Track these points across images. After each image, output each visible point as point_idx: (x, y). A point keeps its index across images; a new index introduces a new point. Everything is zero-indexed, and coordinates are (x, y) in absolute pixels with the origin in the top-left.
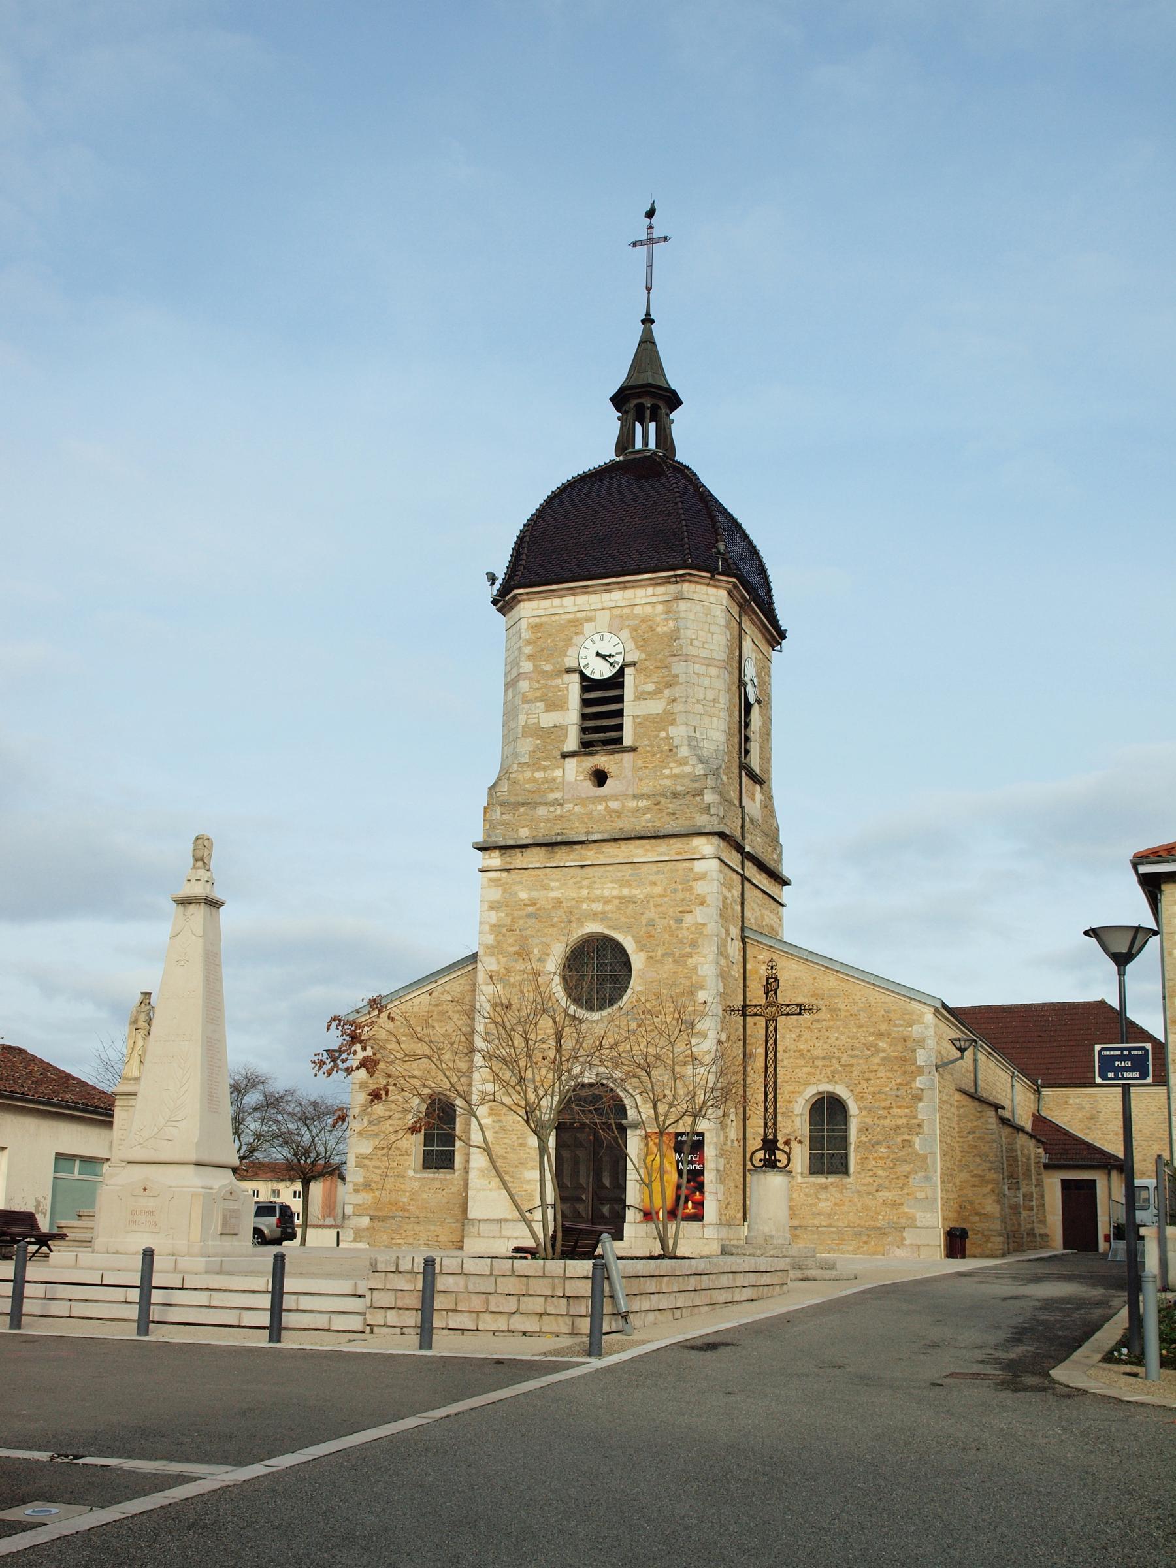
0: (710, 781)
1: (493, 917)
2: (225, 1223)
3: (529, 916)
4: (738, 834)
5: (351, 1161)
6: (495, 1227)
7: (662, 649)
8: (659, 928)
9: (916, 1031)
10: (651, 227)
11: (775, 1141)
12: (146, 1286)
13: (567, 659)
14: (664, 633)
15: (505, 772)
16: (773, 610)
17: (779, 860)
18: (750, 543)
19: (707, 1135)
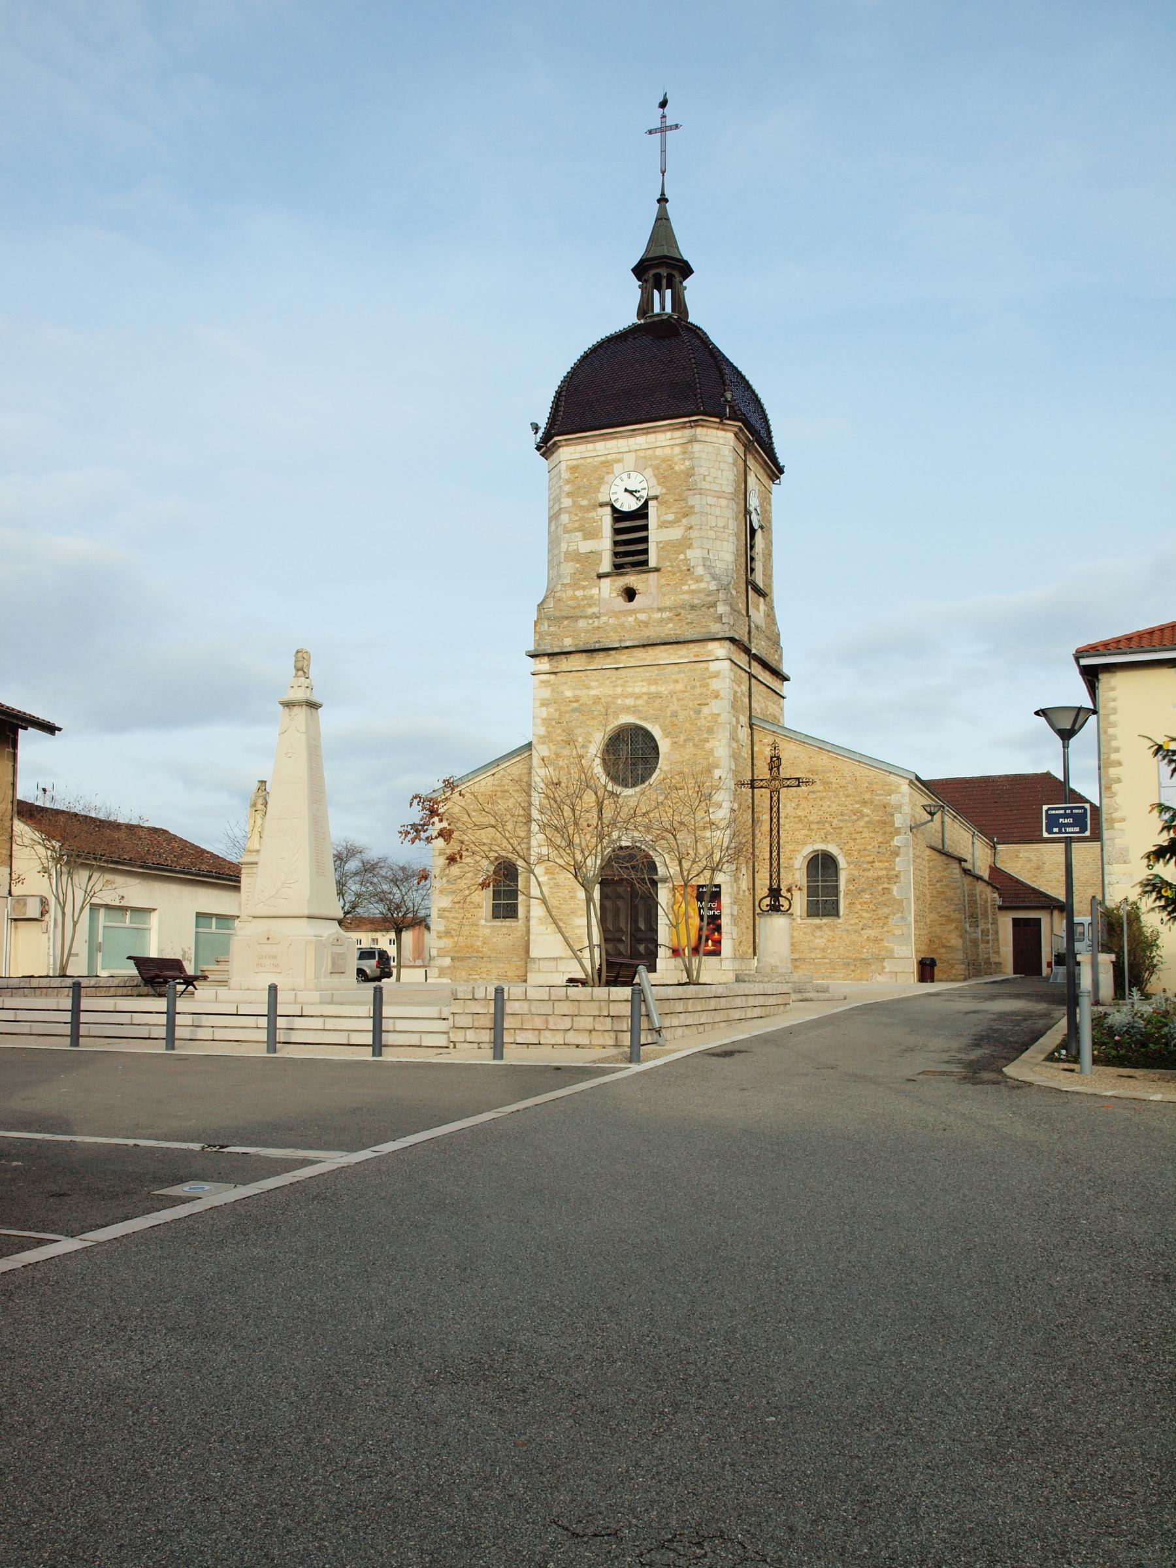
0: (722, 596)
1: (544, 712)
2: (334, 964)
3: (574, 710)
4: (746, 639)
5: (434, 913)
6: (553, 963)
7: (680, 483)
8: (681, 718)
9: (894, 799)
10: (664, 117)
11: (779, 890)
12: (272, 1015)
13: (600, 495)
14: (682, 471)
15: (551, 592)
16: (773, 449)
17: (780, 660)
18: (753, 392)
19: (723, 887)
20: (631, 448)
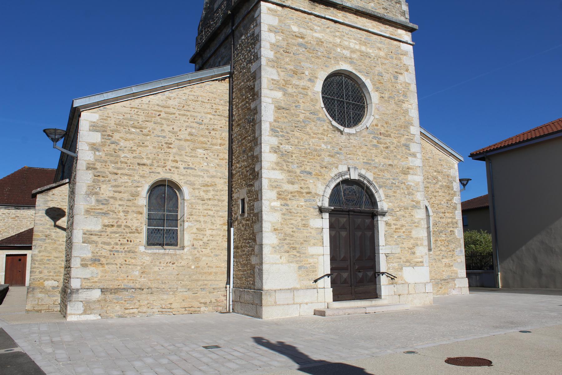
3: (300, 45)
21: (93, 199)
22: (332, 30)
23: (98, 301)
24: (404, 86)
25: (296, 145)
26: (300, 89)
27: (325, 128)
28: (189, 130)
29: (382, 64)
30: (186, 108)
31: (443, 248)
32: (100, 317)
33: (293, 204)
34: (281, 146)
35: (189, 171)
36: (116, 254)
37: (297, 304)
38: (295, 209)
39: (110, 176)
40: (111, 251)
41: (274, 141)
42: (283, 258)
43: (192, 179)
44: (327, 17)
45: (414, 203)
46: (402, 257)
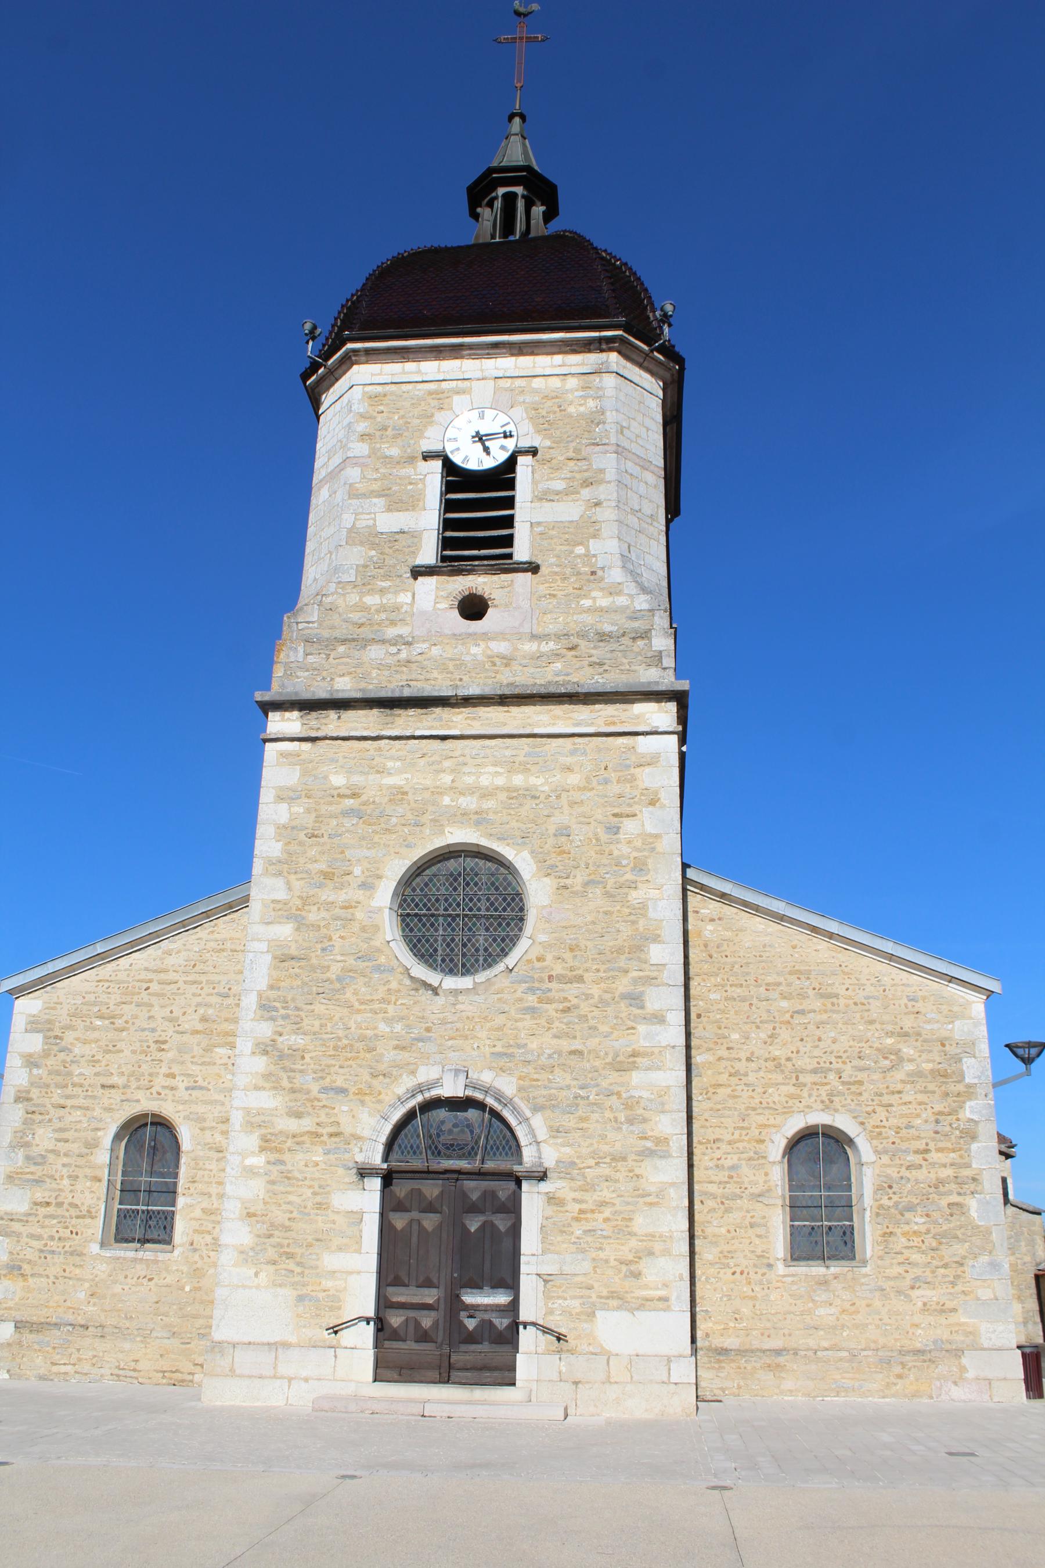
3: (347, 813)
14: (581, 415)
20: (486, 374)
21: (21, 1154)
22: (436, 758)
23: (9, 1345)
24: (638, 843)
25: (314, 1034)
26: (337, 910)
27: (394, 985)
28: (201, 1011)
29: (572, 804)
30: (200, 967)
31: (916, 1257)
32: (7, 1376)
33: (296, 1161)
34: (281, 1039)
35: (195, 1093)
36: (49, 1256)
37: (282, 1377)
38: (301, 1172)
39: (52, 1111)
40: (41, 1251)
41: (265, 1030)
42: (263, 1275)
43: (200, 1109)
44: (418, 733)
45: (649, 1144)
46: (596, 1285)
